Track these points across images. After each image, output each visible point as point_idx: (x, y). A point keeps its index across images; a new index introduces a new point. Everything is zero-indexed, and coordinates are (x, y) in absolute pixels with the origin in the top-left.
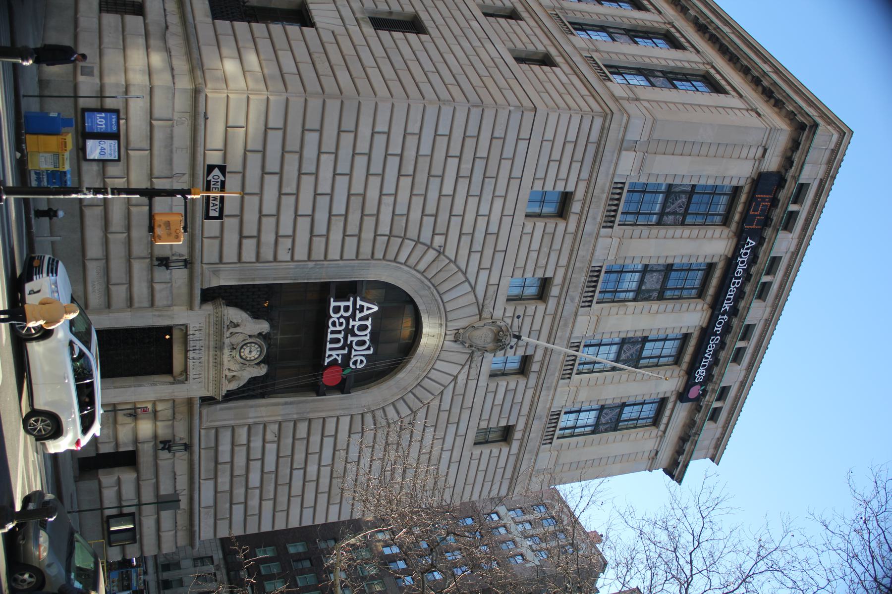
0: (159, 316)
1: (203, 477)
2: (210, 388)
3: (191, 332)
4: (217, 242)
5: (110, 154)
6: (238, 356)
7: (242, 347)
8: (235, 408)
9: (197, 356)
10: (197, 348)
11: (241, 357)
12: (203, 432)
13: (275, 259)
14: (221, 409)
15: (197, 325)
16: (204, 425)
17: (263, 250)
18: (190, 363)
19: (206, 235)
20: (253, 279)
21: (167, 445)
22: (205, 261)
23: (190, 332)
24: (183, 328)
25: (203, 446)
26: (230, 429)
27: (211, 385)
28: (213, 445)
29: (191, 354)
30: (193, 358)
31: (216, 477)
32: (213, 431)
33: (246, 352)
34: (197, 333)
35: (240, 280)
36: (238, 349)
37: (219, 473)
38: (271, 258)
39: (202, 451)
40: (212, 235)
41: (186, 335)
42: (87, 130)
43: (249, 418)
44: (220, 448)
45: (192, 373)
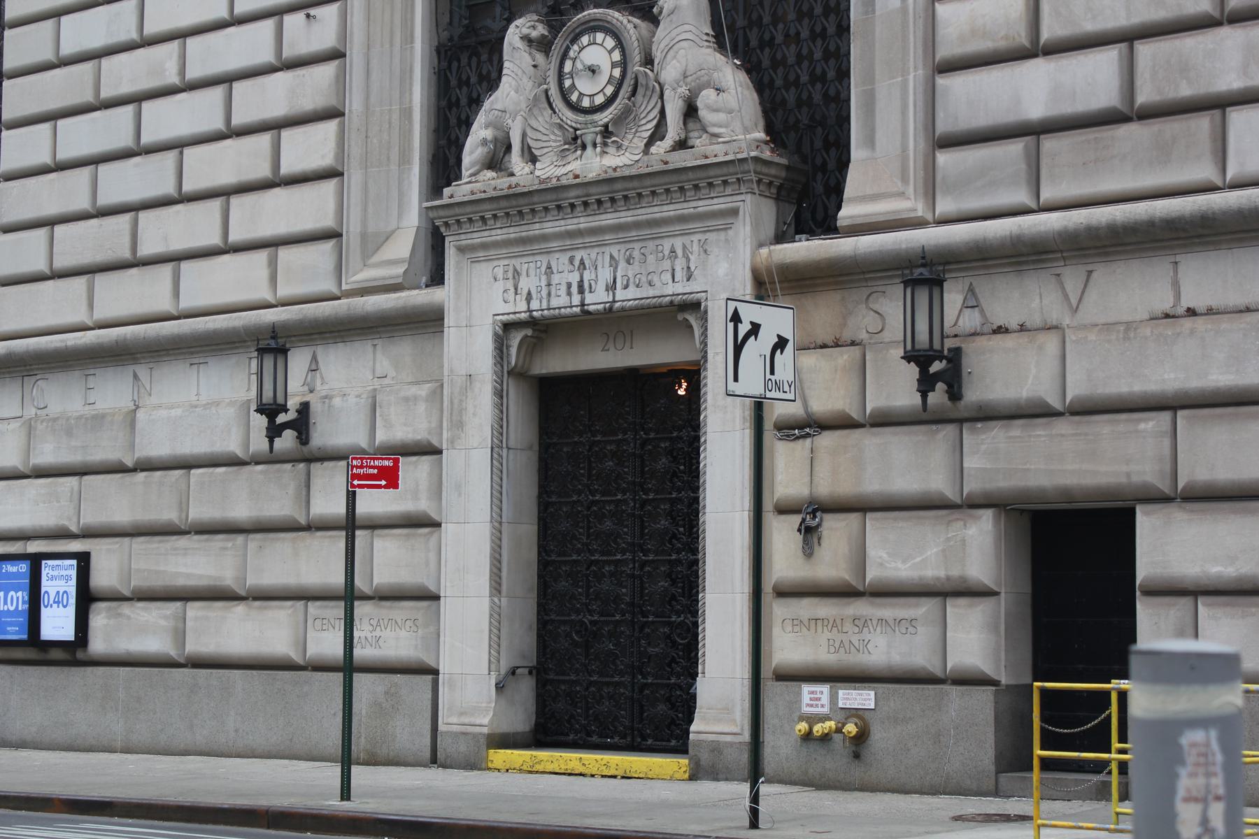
0: (459, 425)
1: (1204, 172)
2: (719, 204)
3: (522, 306)
4: (284, 254)
5: (68, 578)
6: (604, 117)
7: (575, 108)
8: (870, 78)
9: (605, 275)
10: (574, 278)
11: (610, 101)
12: (945, 206)
13: (336, 55)
14: (870, 142)
15: (500, 286)
16: (912, 205)
17: (308, 103)
18: (627, 296)
19: (266, 295)
20: (407, 113)
21: (939, 367)
22: (329, 286)
23: (517, 308)
24: (516, 339)
25: (1021, 197)
26: (941, 81)
27: (704, 206)
28: (1015, 149)
29: (597, 299)
30: (612, 287)
31: (1219, 104)
32: (943, 158)
33: (590, 89)
34: (524, 284)
35: (405, 160)
36: (581, 118)
37: (1186, 91)
38: (327, 71)
39: (1047, 194)
40: (264, 273)
41: (542, 330)
42: (25, 637)
43: (904, 10)
44: (1036, 111)
45: (670, 288)
